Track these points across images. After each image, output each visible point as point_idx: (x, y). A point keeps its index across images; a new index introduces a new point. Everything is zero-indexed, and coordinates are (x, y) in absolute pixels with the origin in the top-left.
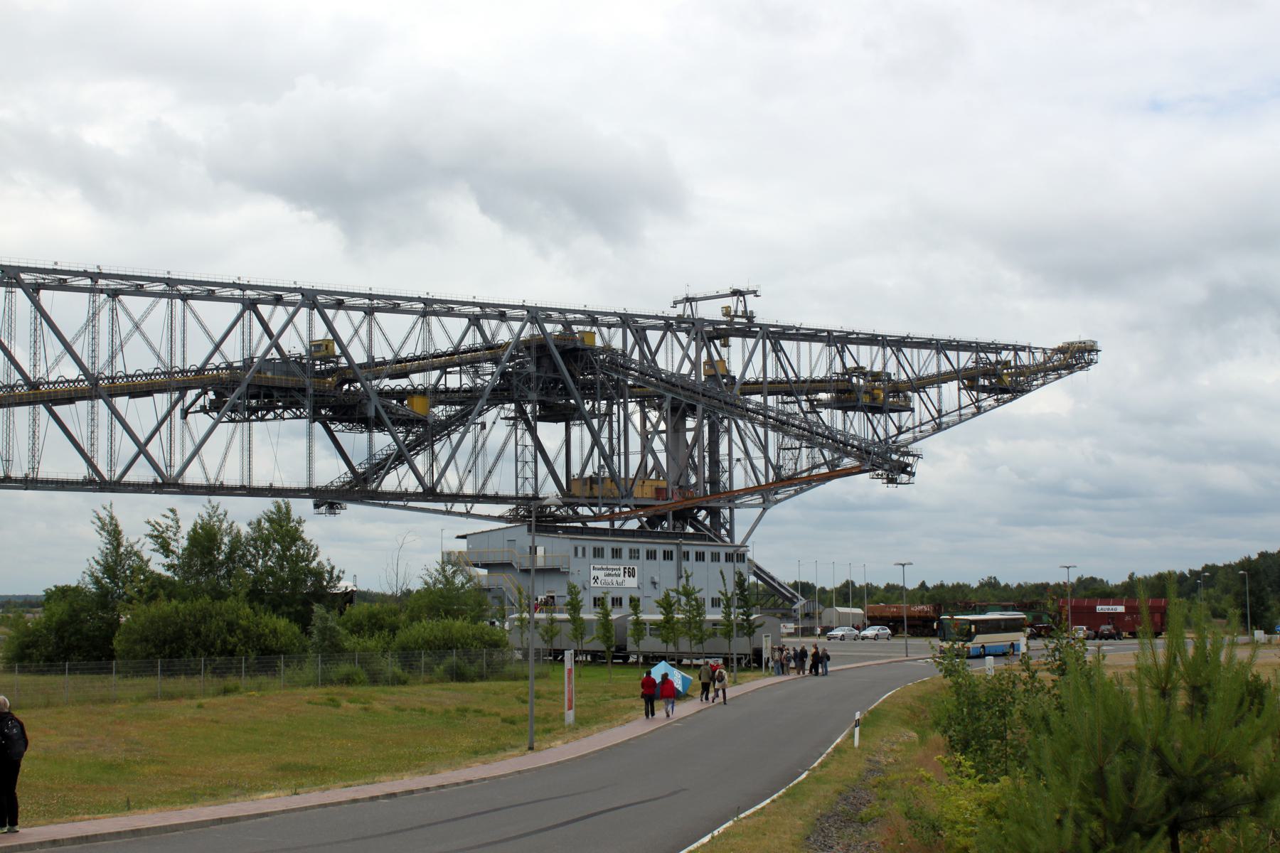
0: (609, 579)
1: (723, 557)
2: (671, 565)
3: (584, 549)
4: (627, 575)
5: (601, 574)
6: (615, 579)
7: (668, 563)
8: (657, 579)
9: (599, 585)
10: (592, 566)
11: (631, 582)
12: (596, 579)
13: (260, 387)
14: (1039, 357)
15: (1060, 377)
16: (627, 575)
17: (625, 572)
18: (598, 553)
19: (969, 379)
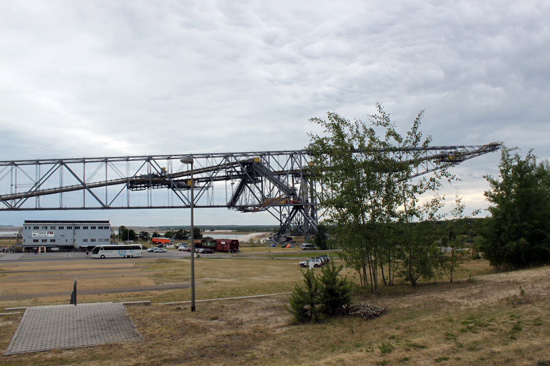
0: (41, 235)
1: (104, 228)
2: (71, 231)
3: (29, 228)
4: (49, 233)
5: (37, 234)
6: (43, 235)
7: (70, 230)
8: (62, 234)
9: (36, 236)
10: (33, 232)
11: (52, 236)
12: (34, 235)
13: (141, 181)
14: (477, 149)
15: (481, 154)
16: (49, 233)
17: (48, 233)
18: (36, 228)
19: (442, 158)
